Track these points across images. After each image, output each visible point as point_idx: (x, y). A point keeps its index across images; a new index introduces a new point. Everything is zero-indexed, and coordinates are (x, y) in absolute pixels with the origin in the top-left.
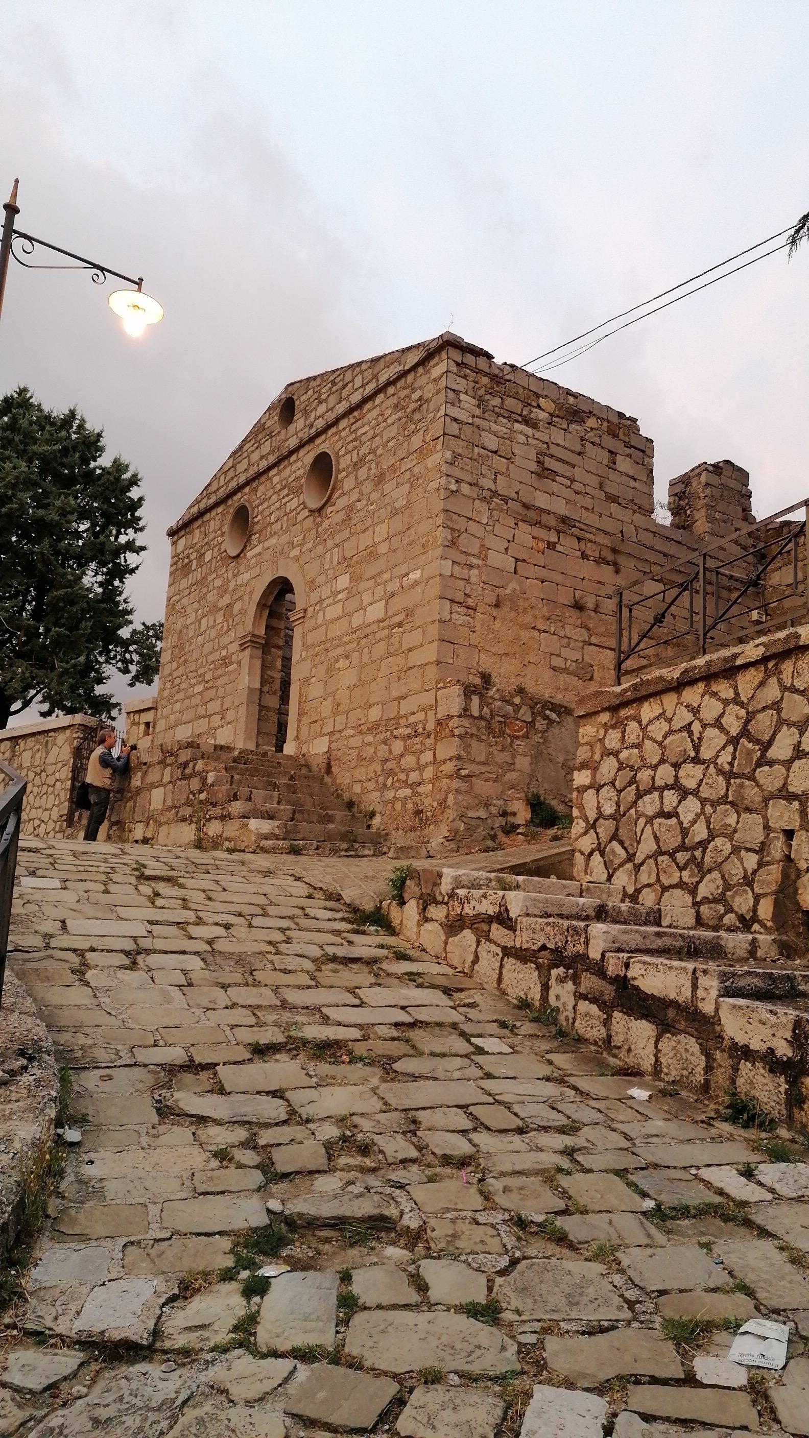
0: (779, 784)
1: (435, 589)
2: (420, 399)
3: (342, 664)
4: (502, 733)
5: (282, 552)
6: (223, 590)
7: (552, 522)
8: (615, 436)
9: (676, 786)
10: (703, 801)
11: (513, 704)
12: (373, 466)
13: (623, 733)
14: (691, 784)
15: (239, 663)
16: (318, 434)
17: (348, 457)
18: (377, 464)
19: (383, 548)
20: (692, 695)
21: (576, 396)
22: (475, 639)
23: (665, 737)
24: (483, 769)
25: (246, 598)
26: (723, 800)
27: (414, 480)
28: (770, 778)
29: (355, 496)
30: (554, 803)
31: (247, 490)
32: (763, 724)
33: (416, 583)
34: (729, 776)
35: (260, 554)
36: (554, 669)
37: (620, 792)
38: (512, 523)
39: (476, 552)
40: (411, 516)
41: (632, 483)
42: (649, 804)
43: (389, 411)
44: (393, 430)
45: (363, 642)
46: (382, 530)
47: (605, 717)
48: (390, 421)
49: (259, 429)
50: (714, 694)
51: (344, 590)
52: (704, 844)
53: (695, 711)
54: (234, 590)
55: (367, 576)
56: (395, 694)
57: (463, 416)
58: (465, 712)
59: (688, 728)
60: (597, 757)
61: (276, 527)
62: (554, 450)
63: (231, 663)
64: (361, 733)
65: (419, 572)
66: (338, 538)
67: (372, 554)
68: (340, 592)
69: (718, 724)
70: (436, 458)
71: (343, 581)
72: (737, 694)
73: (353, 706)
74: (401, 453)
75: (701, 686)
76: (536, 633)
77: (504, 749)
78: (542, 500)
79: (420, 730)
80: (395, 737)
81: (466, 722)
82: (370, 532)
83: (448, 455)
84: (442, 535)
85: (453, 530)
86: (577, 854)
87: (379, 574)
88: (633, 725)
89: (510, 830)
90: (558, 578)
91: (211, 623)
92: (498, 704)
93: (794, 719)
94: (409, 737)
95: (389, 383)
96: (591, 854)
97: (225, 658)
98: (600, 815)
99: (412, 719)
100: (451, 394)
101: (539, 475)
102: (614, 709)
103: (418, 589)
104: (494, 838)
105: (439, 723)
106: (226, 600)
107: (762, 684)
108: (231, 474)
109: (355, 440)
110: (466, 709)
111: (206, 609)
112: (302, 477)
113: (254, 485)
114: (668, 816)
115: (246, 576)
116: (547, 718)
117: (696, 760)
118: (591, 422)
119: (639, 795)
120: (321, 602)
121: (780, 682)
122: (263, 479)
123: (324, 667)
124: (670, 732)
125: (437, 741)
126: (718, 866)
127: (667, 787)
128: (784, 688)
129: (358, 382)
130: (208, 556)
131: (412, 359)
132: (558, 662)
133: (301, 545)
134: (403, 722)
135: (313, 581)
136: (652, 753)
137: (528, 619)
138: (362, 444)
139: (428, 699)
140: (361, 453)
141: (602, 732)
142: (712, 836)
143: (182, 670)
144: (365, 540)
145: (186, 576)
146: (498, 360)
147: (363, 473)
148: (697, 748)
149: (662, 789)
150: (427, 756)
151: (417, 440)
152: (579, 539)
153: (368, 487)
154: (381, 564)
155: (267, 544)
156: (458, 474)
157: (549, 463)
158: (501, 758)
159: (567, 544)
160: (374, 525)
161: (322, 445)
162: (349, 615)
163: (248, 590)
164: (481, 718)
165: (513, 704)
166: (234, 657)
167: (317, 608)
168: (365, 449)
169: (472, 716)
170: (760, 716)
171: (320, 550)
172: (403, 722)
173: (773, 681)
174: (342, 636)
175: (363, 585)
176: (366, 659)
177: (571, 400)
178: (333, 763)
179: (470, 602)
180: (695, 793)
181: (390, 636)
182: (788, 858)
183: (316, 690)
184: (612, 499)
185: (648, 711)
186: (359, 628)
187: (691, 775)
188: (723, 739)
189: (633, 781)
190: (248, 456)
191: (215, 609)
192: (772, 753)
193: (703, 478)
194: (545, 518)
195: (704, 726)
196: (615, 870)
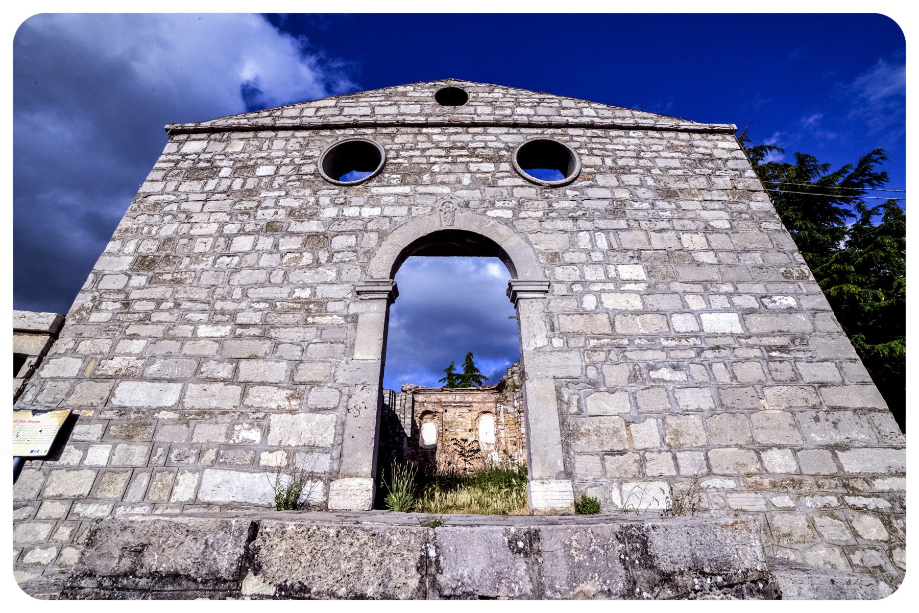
35: (406, 196)
43: (661, 148)
61: (452, 178)
66: (602, 224)
140: (621, 162)
147: (631, 179)
155: (421, 189)
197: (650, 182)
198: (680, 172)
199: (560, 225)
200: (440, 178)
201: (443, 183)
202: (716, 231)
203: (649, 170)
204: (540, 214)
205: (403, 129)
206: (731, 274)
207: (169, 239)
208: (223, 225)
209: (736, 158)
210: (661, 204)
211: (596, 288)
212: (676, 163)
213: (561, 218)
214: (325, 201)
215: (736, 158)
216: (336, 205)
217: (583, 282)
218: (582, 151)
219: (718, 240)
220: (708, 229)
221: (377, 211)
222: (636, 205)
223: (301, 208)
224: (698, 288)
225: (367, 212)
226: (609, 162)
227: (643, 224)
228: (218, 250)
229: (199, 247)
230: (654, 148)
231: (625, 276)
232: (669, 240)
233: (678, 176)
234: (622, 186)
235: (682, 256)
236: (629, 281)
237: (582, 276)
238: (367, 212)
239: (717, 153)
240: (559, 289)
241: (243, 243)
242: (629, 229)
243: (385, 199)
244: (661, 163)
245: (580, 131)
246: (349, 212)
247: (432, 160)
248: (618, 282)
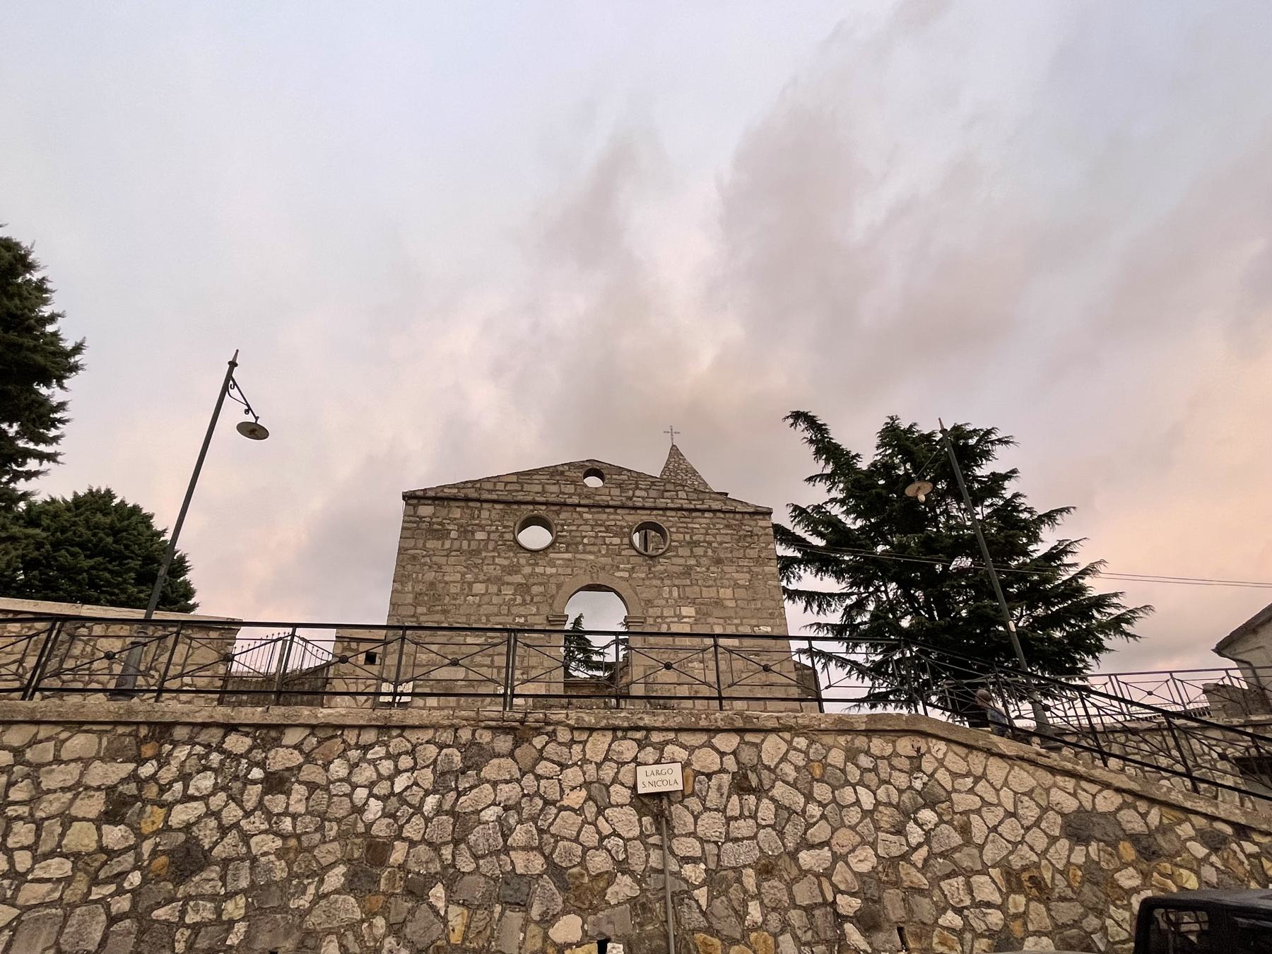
2: (751, 532)
35: (570, 560)
44: (728, 539)
51: (690, 617)
61: (595, 549)
66: (677, 582)
68: (686, 617)
130: (480, 535)
131: (740, 508)
140: (694, 538)
147: (699, 551)
151: (752, 553)
155: (578, 556)
197: (710, 553)
198: (729, 545)
199: (655, 582)
200: (589, 548)
201: (590, 553)
202: (740, 587)
203: (710, 543)
204: (643, 575)
205: (565, 508)
206: (741, 613)
207: (432, 584)
208: (463, 575)
209: (767, 535)
210: (712, 569)
211: (668, 620)
212: (728, 539)
213: (655, 578)
214: (523, 561)
215: (767, 535)
216: (530, 565)
217: (662, 617)
218: (672, 530)
220: (736, 585)
221: (554, 570)
222: (698, 569)
223: (509, 566)
224: (721, 621)
225: (549, 570)
226: (688, 537)
227: (700, 582)
228: (465, 592)
229: (453, 590)
230: (718, 526)
231: (684, 614)
232: (712, 593)
233: (727, 548)
234: (692, 555)
235: (718, 603)
236: (686, 617)
237: (662, 613)
238: (549, 570)
239: (756, 530)
240: (650, 621)
241: (479, 588)
242: (692, 585)
243: (558, 562)
244: (719, 539)
245: (673, 513)
246: (539, 570)
247: (584, 534)
248: (680, 617)
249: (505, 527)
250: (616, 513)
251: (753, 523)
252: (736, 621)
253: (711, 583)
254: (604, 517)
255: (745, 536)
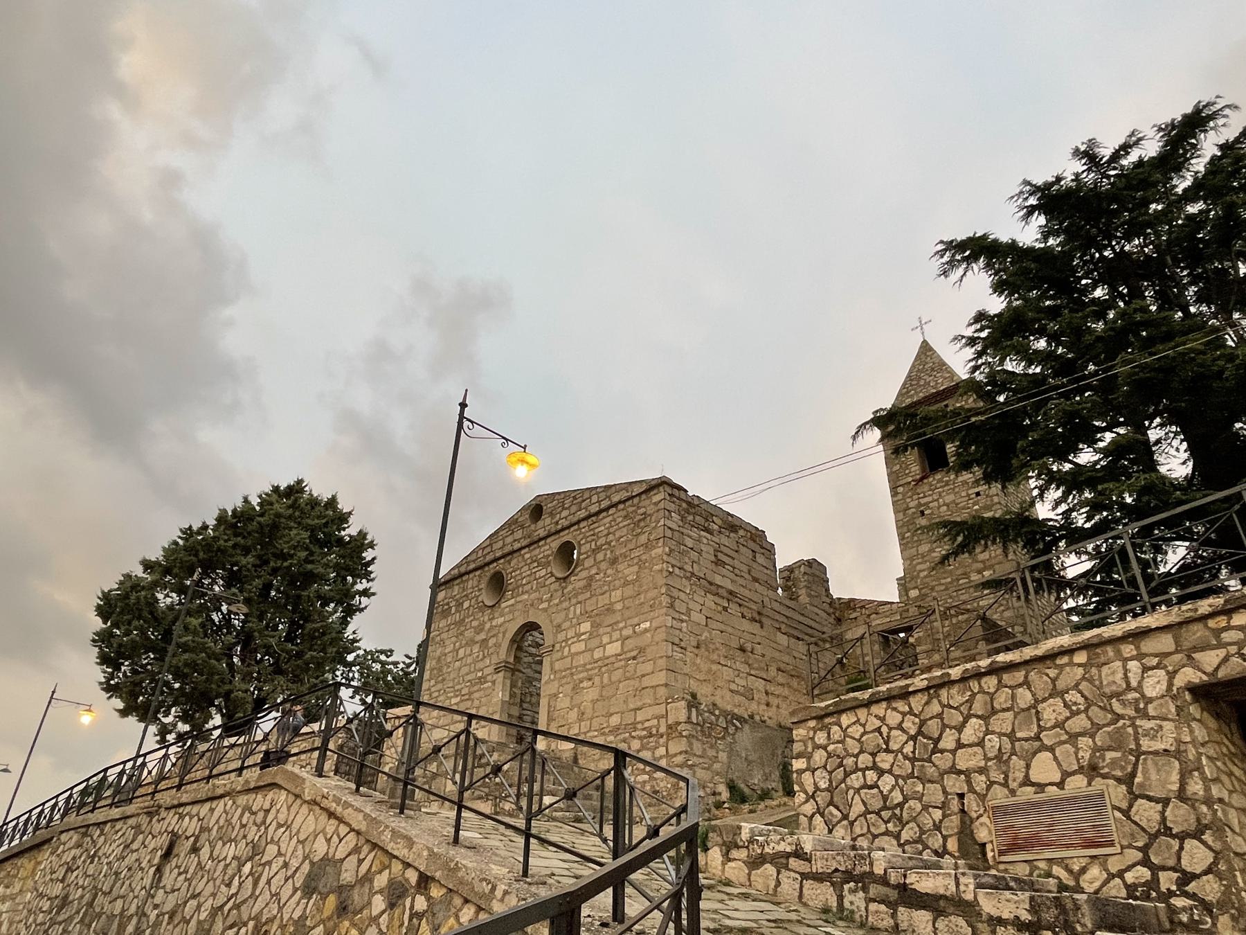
0: (949, 764)
1: (661, 635)
2: (645, 513)
3: (585, 684)
4: (710, 735)
5: (532, 605)
6: (479, 630)
7: (725, 594)
8: (755, 541)
9: (874, 767)
10: (897, 777)
11: (715, 715)
12: (608, 552)
13: (829, 734)
14: (886, 766)
15: (494, 682)
16: (563, 529)
17: (588, 545)
18: (612, 552)
19: (618, 606)
20: (879, 709)
21: (732, 516)
22: (687, 670)
23: (862, 736)
24: (701, 760)
25: (501, 635)
26: (911, 776)
27: (641, 564)
28: (943, 761)
29: (594, 571)
30: (742, 786)
31: (502, 561)
32: (933, 727)
33: (646, 630)
34: (913, 760)
35: (512, 605)
36: (732, 691)
37: (830, 773)
38: (703, 594)
39: (684, 611)
40: (640, 586)
41: (765, 571)
42: (855, 780)
43: (621, 519)
45: (603, 669)
46: (617, 595)
47: (812, 724)
48: (621, 525)
49: (511, 524)
50: (895, 709)
52: (901, 805)
53: (883, 719)
54: (489, 630)
55: (606, 624)
56: (632, 706)
57: (674, 526)
58: (689, 721)
59: (878, 730)
60: (810, 749)
61: (527, 588)
62: (723, 548)
63: (485, 682)
64: (603, 734)
65: (648, 624)
66: (581, 598)
67: (609, 610)
68: (583, 634)
69: (900, 727)
70: (659, 551)
71: (586, 627)
72: (911, 708)
73: (596, 714)
74: (631, 546)
75: (884, 704)
76: (720, 667)
77: (712, 747)
78: (718, 580)
79: (654, 732)
80: (634, 737)
81: (689, 727)
82: (607, 595)
83: (667, 549)
84: (665, 600)
85: (671, 597)
86: (801, 817)
87: (618, 622)
88: (835, 728)
89: (719, 805)
90: (730, 630)
91: (468, 652)
92: (707, 714)
93: (953, 724)
94: (645, 737)
95: (620, 502)
96: (813, 815)
97: (480, 678)
98: (817, 789)
99: (647, 724)
100: (667, 512)
101: (716, 564)
102: (820, 718)
103: (648, 635)
104: (709, 811)
105: (669, 727)
106: (482, 636)
107: (927, 703)
108: (488, 549)
109: (593, 535)
110: (689, 718)
111: (464, 642)
112: (549, 556)
113: (508, 558)
114: (871, 787)
115: (501, 620)
116: (734, 725)
117: (888, 751)
118: (741, 532)
119: (847, 774)
120: (566, 640)
121: (940, 702)
122: (515, 555)
123: (571, 686)
124: (865, 733)
125: (668, 740)
126: (914, 819)
127: (867, 768)
128: (943, 706)
129: (595, 499)
130: (466, 605)
131: (637, 490)
132: (733, 687)
133: (549, 601)
134: (639, 726)
135: (559, 626)
136: (853, 747)
137: (715, 657)
138: (599, 538)
139: (660, 710)
141: (811, 733)
142: (906, 800)
143: (439, 686)
144: (603, 601)
145: (445, 617)
146: (690, 494)
147: (600, 556)
148: (887, 743)
149: (864, 770)
150: (662, 751)
151: (643, 539)
152: (740, 605)
153: (603, 566)
154: (618, 617)
155: (518, 599)
156: (674, 562)
157: (720, 556)
158: (711, 753)
159: (733, 608)
160: (611, 591)
161: (566, 537)
162: (592, 650)
163: (502, 629)
164: (698, 724)
165: (715, 715)
166: (489, 678)
167: (563, 644)
168: (602, 541)
169: (692, 723)
170: (929, 723)
171: (565, 605)
172: (639, 726)
173: (935, 701)
174: (585, 665)
175: (601, 631)
176: (606, 681)
177: (730, 518)
178: (579, 757)
179: (683, 644)
180: (890, 772)
181: (627, 666)
182: (963, 811)
183: (563, 702)
184: (756, 580)
185: (845, 720)
186: (600, 659)
187: (885, 761)
188: (905, 738)
189: (841, 765)
190: (503, 539)
191: (472, 642)
192: (941, 745)
193: (802, 569)
194: (720, 591)
195: (890, 729)
196: (834, 826)
203: (609, 543)
219: (629, 591)
222: (598, 577)
224: (609, 629)
242: (592, 596)
249: (480, 590)
250: (546, 544)
251: (647, 502)
252: (621, 625)
253: (606, 588)
254: (537, 551)
255: (640, 521)
